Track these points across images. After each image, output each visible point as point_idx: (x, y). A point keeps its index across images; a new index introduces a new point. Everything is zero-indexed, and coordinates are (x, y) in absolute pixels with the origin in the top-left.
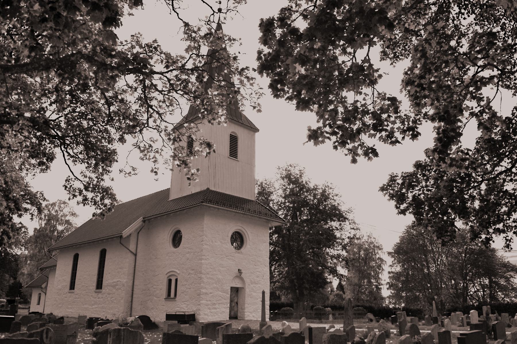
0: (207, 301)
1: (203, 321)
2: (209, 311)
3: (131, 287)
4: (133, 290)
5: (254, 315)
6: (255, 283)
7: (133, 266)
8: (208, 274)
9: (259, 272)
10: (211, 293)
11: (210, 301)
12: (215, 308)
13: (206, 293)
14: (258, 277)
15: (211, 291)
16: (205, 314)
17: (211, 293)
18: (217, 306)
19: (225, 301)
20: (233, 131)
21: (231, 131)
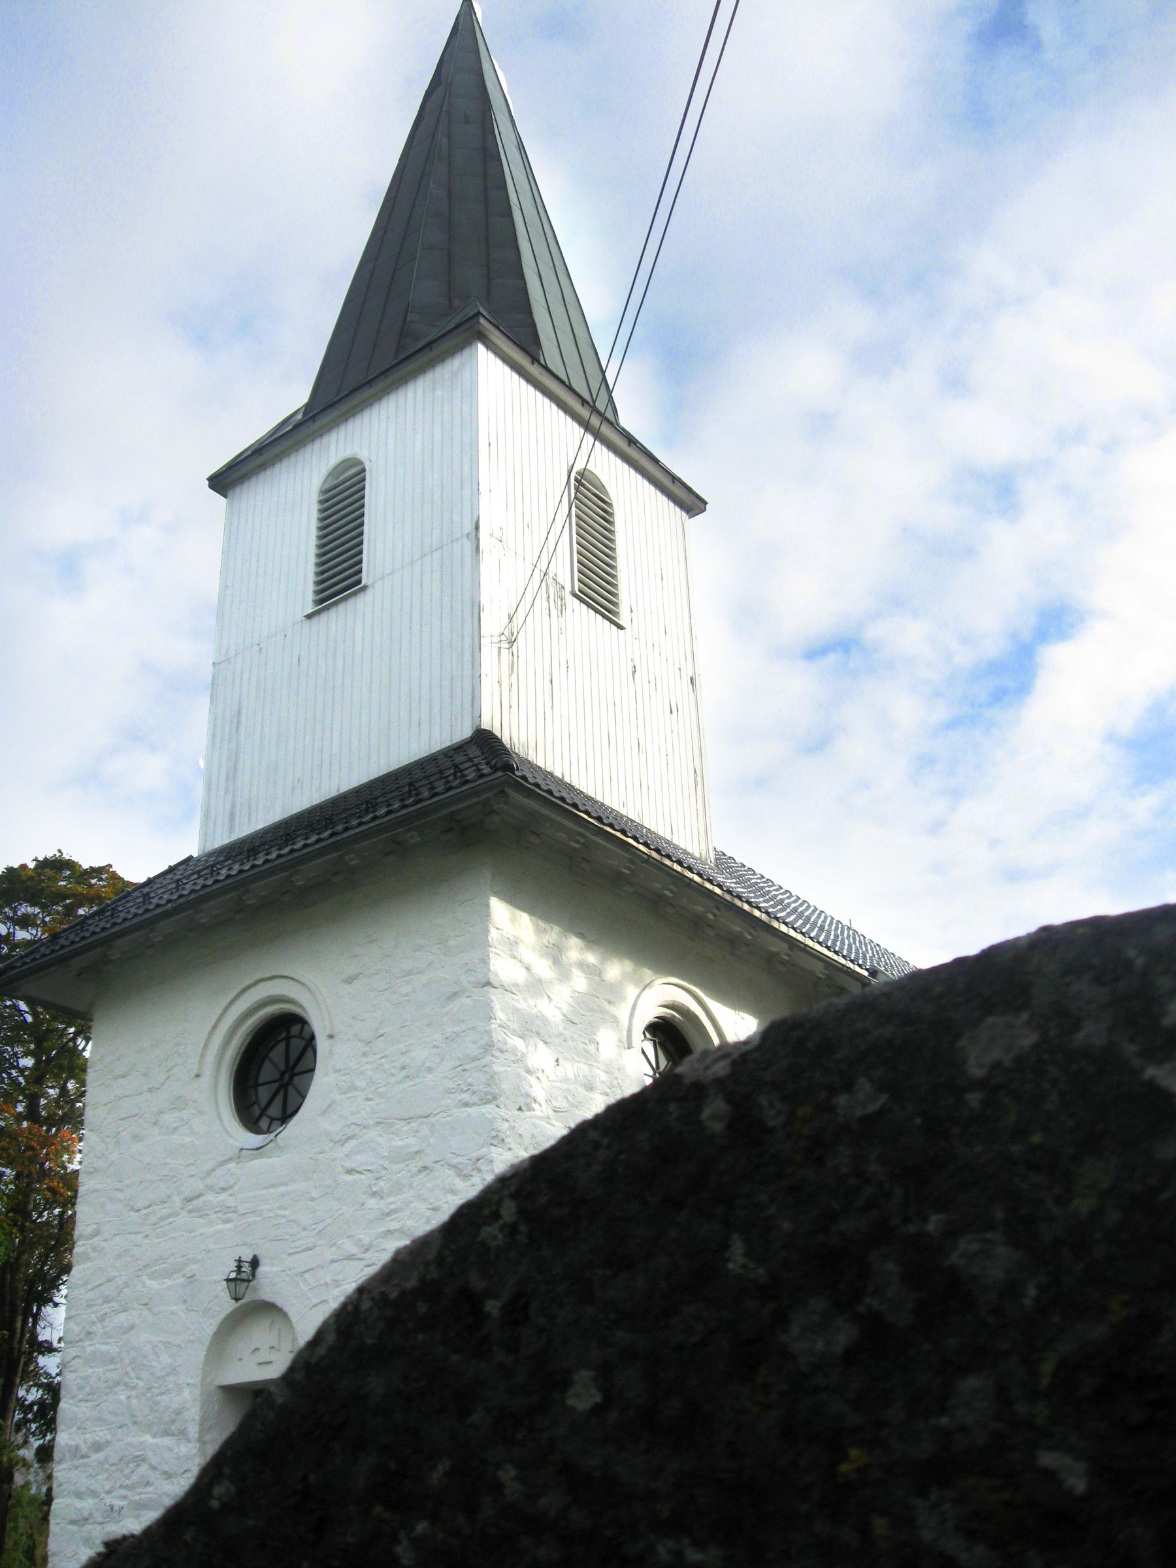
11: (94, 1494)
17: (97, 1447)
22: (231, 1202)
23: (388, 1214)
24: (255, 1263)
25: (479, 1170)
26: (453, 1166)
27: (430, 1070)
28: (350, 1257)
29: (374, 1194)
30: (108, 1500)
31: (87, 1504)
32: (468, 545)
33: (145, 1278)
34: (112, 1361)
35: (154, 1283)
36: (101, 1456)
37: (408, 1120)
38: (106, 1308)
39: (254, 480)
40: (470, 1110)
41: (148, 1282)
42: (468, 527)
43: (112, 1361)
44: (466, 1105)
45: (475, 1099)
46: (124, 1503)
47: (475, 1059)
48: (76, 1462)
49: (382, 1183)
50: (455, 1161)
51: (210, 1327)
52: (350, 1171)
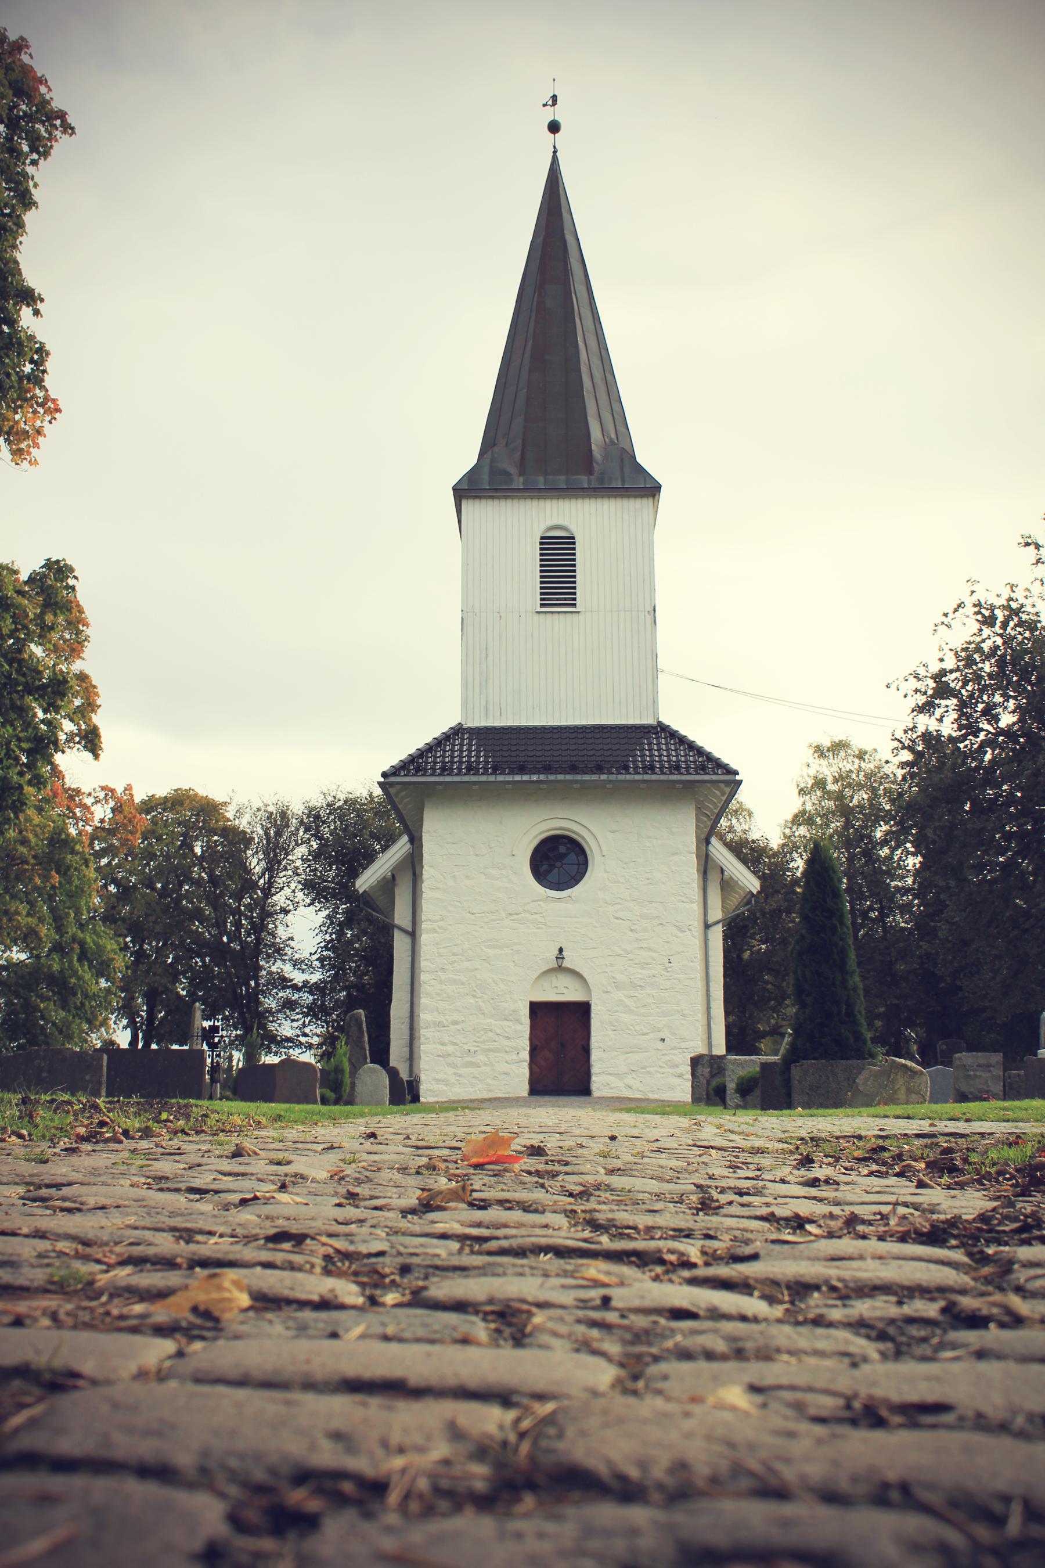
0: (442, 1044)
1: (431, 1099)
2: (451, 1071)
3: (408, 1020)
4: (412, 1028)
5: (629, 1080)
6: (635, 986)
7: (409, 965)
9: (650, 949)
10: (455, 1023)
13: (439, 1024)
15: (456, 1017)
16: (438, 1081)
17: (455, 1023)
18: (481, 1058)
19: (505, 1042)
20: (550, 523)
22: (542, 920)
24: (561, 950)
25: (690, 930)
27: (663, 883)
28: (618, 955)
30: (466, 1047)
31: (450, 1048)
32: (649, 619)
33: (483, 947)
34: (463, 984)
35: (489, 951)
36: (459, 1027)
37: (651, 902)
38: (455, 958)
39: (484, 501)
41: (485, 950)
42: (650, 608)
43: (463, 984)
45: (687, 900)
46: (476, 1049)
47: (689, 884)
48: (438, 1029)
49: (637, 927)
50: (677, 924)
52: (617, 918)
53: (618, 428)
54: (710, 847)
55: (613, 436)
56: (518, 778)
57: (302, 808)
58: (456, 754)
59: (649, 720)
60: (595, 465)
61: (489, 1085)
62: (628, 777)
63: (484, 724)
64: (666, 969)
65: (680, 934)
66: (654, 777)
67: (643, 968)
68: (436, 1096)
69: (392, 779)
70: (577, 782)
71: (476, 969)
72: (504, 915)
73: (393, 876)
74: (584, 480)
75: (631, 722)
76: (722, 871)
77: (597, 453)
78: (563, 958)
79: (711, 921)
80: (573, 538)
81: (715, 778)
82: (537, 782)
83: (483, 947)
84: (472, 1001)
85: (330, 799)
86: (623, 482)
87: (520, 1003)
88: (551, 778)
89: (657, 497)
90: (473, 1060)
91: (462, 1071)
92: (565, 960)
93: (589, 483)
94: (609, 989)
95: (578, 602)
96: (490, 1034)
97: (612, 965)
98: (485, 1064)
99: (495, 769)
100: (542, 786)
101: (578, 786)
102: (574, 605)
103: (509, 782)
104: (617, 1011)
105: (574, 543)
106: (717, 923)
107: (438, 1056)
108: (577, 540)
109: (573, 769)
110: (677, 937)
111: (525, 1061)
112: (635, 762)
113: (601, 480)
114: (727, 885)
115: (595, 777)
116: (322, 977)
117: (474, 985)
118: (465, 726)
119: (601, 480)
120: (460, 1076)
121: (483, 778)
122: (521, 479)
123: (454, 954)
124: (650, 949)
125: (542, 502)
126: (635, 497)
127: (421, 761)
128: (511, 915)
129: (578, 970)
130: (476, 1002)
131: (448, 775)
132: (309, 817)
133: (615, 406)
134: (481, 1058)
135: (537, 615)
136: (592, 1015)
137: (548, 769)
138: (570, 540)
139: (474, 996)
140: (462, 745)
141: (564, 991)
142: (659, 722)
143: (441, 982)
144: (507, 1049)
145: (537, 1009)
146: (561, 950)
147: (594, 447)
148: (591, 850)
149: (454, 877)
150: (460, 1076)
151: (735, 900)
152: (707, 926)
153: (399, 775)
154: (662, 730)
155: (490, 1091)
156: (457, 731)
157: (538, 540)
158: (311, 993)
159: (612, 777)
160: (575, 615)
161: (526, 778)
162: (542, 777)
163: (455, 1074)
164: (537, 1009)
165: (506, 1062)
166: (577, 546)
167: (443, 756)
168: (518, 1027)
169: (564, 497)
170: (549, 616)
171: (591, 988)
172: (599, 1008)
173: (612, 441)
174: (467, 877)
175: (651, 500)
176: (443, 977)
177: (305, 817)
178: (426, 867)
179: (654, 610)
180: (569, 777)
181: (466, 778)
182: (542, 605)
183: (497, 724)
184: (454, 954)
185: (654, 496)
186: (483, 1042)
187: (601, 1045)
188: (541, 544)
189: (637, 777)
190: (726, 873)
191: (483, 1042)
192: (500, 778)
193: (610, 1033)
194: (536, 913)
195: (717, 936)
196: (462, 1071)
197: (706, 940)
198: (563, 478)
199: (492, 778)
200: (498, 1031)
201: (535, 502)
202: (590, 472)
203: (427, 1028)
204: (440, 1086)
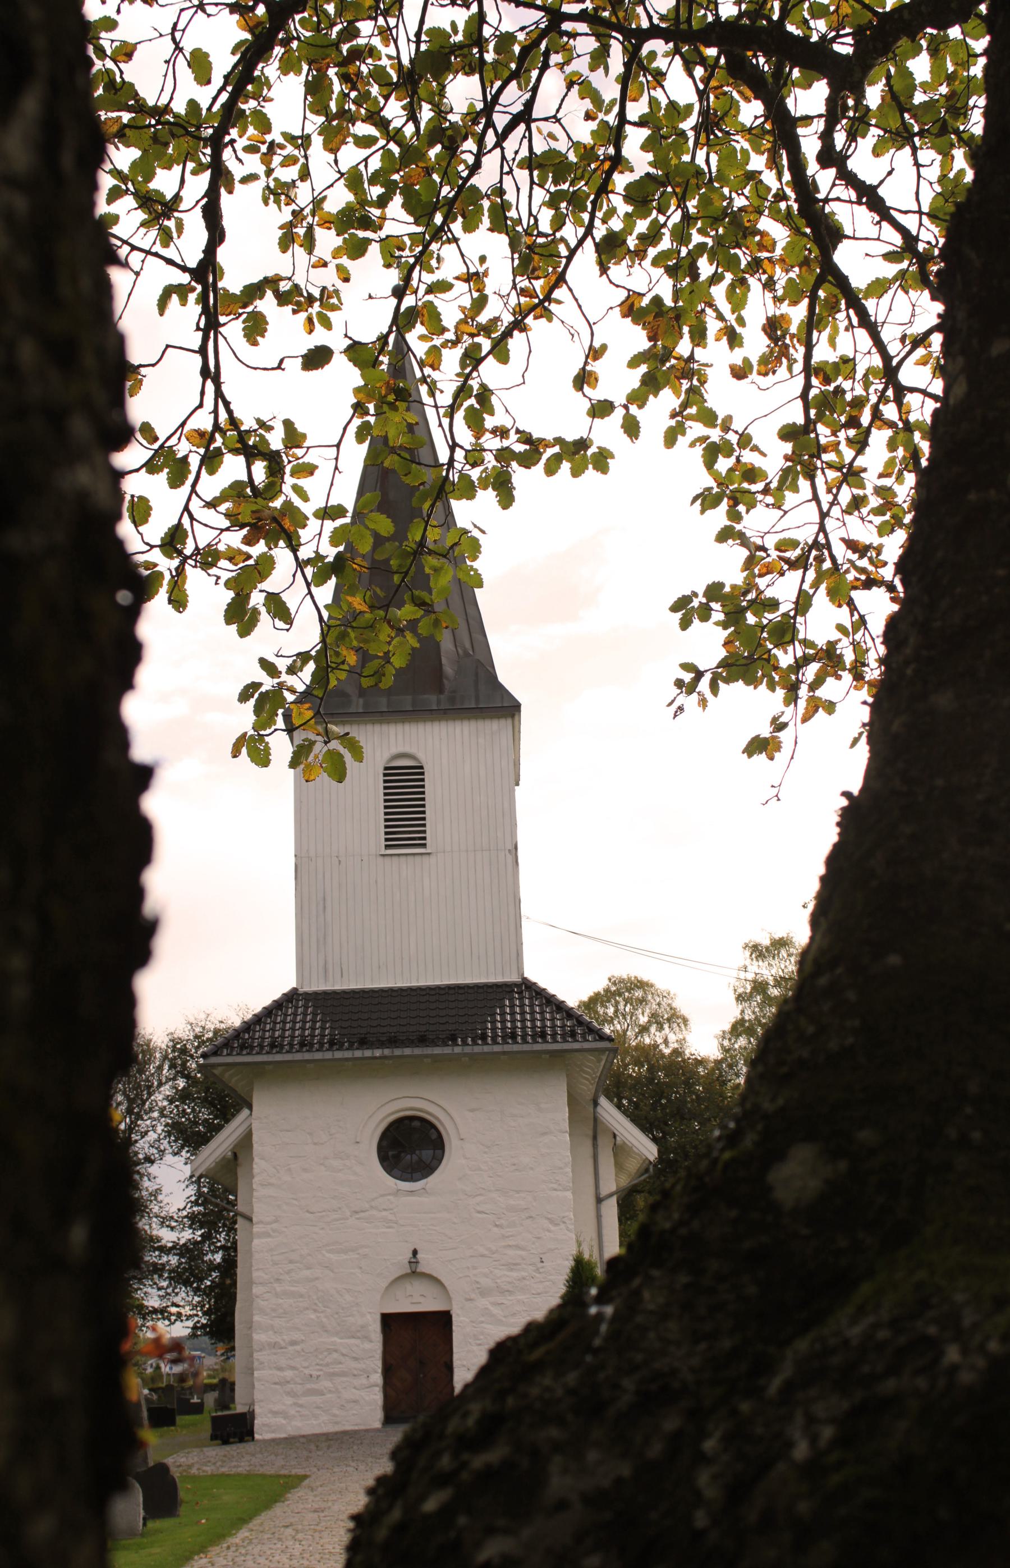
0: (280, 1369)
1: (268, 1436)
2: (289, 1400)
6: (503, 1292)
8: (278, 1280)
9: (518, 1247)
10: (293, 1343)
11: (293, 1368)
12: (321, 1393)
13: (275, 1345)
14: (512, 1266)
15: (296, 1336)
16: (275, 1413)
17: (293, 1343)
19: (354, 1364)
20: (394, 751)
21: (387, 756)
22: (391, 1217)
23: (508, 1237)
24: (415, 1253)
25: (564, 1222)
26: (548, 1219)
27: (532, 1169)
28: (483, 1256)
29: (496, 1226)
30: (307, 1372)
31: (289, 1374)
32: (510, 858)
33: (324, 1252)
34: (301, 1296)
35: (331, 1256)
36: (298, 1348)
37: (518, 1192)
38: (291, 1266)
40: (559, 1193)
41: (327, 1255)
42: (509, 846)
43: (301, 1296)
44: (555, 1190)
48: (274, 1351)
50: (549, 1216)
51: (384, 1284)
52: (479, 1212)
53: (474, 635)
54: (599, 1109)
55: (468, 645)
56: (358, 1054)
57: (166, 1040)
58: (288, 1026)
59: (514, 978)
60: (445, 681)
61: (335, 1415)
62: (486, 1049)
63: (322, 987)
64: (538, 1269)
65: (553, 1228)
66: (515, 1048)
67: (512, 1270)
68: (273, 1432)
69: (213, 1060)
70: (427, 1056)
71: (317, 1279)
72: (348, 1214)
73: (235, 1155)
74: (432, 700)
75: (492, 979)
76: (615, 1136)
77: (448, 669)
78: (417, 1262)
79: (604, 1191)
80: (422, 767)
81: (586, 1045)
82: (380, 1058)
83: (324, 1252)
84: (313, 1316)
85: (198, 1030)
86: (477, 701)
87: (369, 1317)
88: (398, 1052)
89: (516, 717)
90: (313, 1386)
91: (302, 1400)
92: (419, 1265)
93: (439, 702)
94: (473, 1296)
95: (428, 842)
96: (335, 1355)
97: (475, 1268)
98: (330, 1391)
99: (332, 1043)
100: (386, 1062)
101: (429, 1060)
102: (424, 845)
103: (347, 1059)
104: (482, 1322)
105: (423, 774)
106: (611, 1195)
107: (275, 1383)
108: (426, 770)
109: (423, 1040)
110: (549, 1231)
111: (377, 1385)
112: (494, 1029)
113: (452, 700)
114: (620, 1151)
115: (447, 1050)
116: (191, 1236)
117: (315, 1297)
118: (301, 991)
119: (452, 700)
120: (301, 1406)
121: (318, 1056)
122: (361, 701)
123: (291, 1262)
124: (518, 1247)
125: (385, 727)
126: (491, 718)
127: (247, 1036)
128: (356, 1212)
129: (435, 1274)
130: (318, 1317)
131: (277, 1052)
132: (173, 1051)
133: (470, 611)
134: (326, 1384)
135: (381, 859)
136: (454, 1328)
137: (393, 1042)
138: (418, 771)
139: (315, 1311)
140: (295, 1014)
141: (421, 1300)
142: (525, 979)
143: (277, 1295)
144: (355, 1372)
145: (389, 1321)
146: (415, 1253)
147: (444, 661)
148: (448, 1134)
149: (289, 1170)
150: (301, 1406)
151: (633, 1166)
152: (599, 1200)
153: (220, 1055)
154: (529, 989)
155: (337, 1423)
156: (291, 997)
157: (381, 771)
158: (181, 1255)
159: (468, 1049)
160: (425, 858)
161: (368, 1053)
162: (387, 1052)
163: (295, 1404)
164: (389, 1321)
165: (355, 1388)
166: (426, 777)
167: (273, 1030)
168: (367, 1346)
169: (410, 721)
170: (395, 859)
171: (452, 1295)
172: (462, 1318)
173: (466, 654)
174: (305, 1170)
175: (509, 721)
176: (278, 1289)
177: (170, 1051)
178: (256, 1160)
179: (516, 848)
180: (417, 1051)
181: (298, 1056)
182: (387, 847)
183: (338, 987)
184: (291, 1262)
185: (513, 716)
186: (327, 1365)
187: (465, 1363)
188: (385, 775)
189: (497, 1048)
190: (618, 1138)
191: (327, 1365)
192: (339, 1055)
193: (475, 1348)
194: (385, 1210)
195: (611, 1210)
196: (302, 1400)
197: (599, 1217)
198: (409, 698)
199: (328, 1055)
200: (344, 1351)
201: (377, 728)
202: (441, 691)
203: (261, 1350)
204: (277, 1420)
